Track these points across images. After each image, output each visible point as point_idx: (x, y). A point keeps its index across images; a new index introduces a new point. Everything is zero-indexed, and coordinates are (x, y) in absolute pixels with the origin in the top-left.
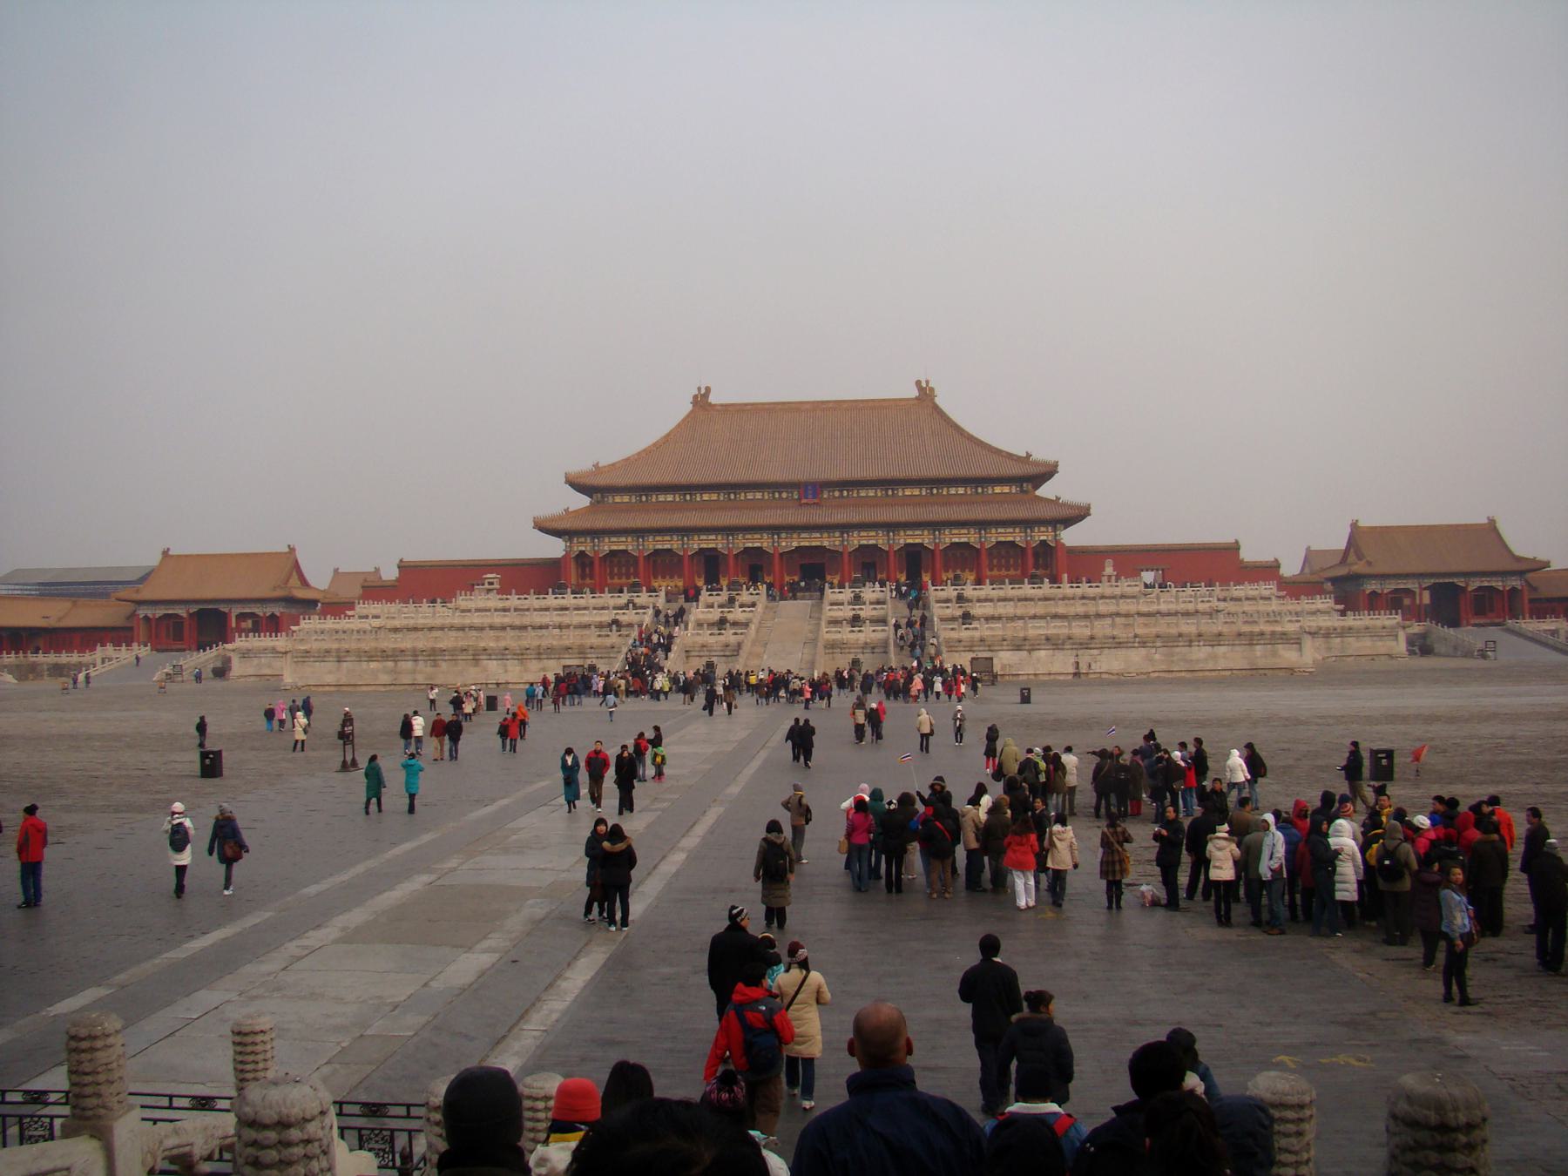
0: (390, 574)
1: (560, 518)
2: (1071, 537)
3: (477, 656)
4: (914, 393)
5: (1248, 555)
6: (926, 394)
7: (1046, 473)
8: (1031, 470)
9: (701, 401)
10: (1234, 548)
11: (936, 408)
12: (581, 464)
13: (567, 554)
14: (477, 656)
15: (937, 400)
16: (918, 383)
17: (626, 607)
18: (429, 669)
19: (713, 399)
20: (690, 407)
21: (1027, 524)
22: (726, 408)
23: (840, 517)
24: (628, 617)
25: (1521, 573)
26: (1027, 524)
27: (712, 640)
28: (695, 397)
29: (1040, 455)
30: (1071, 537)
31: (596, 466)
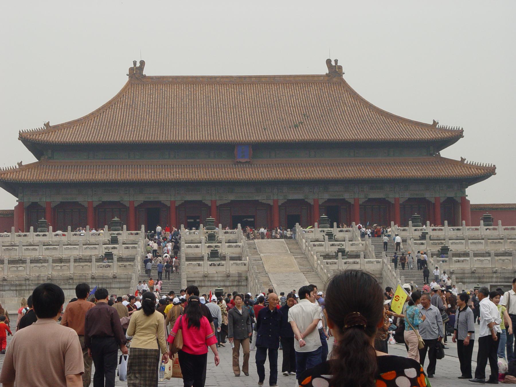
1: (13, 171)
2: (476, 194)
4: (324, 70)
6: (335, 71)
8: (440, 135)
11: (344, 82)
12: (34, 124)
13: (21, 204)
15: (344, 77)
16: (329, 62)
17: (114, 241)
19: (147, 72)
20: (127, 79)
24: (119, 251)
27: (212, 271)
28: (131, 69)
29: (448, 121)
30: (476, 194)
31: (47, 125)
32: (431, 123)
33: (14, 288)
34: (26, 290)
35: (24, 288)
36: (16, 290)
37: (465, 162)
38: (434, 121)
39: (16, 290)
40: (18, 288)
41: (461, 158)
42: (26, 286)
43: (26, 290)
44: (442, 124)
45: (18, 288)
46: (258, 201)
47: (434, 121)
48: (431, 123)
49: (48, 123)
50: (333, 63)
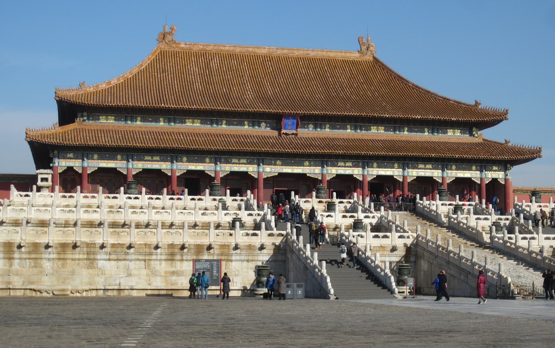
7: (493, 119)
21: (484, 164)
29: (489, 103)
32: (473, 103)
33: (143, 258)
34: (156, 260)
35: (154, 257)
36: (145, 260)
37: (510, 144)
38: (476, 102)
39: (145, 260)
40: (147, 258)
41: (506, 141)
42: (157, 255)
43: (156, 260)
45: (147, 258)
46: (305, 174)
47: (476, 102)
48: (474, 103)
49: (83, 83)
50: (365, 40)
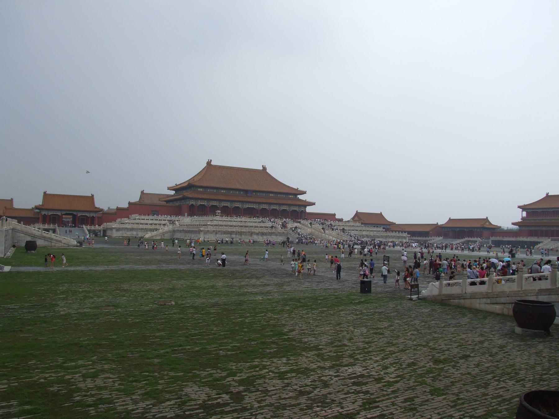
0: (126, 206)
2: (309, 209)
3: (251, 234)
5: (337, 217)
6: (264, 168)
9: (209, 163)
10: (335, 215)
14: (251, 234)
18: (240, 237)
19: (212, 163)
20: (206, 165)
22: (215, 166)
23: (258, 200)
25: (389, 225)
26: (299, 206)
30: (309, 209)
44: (300, 189)
